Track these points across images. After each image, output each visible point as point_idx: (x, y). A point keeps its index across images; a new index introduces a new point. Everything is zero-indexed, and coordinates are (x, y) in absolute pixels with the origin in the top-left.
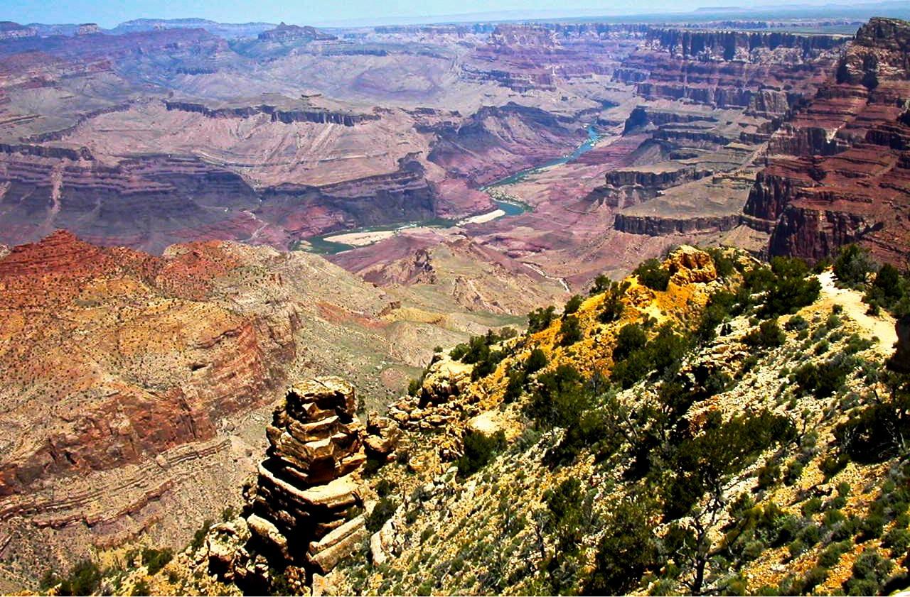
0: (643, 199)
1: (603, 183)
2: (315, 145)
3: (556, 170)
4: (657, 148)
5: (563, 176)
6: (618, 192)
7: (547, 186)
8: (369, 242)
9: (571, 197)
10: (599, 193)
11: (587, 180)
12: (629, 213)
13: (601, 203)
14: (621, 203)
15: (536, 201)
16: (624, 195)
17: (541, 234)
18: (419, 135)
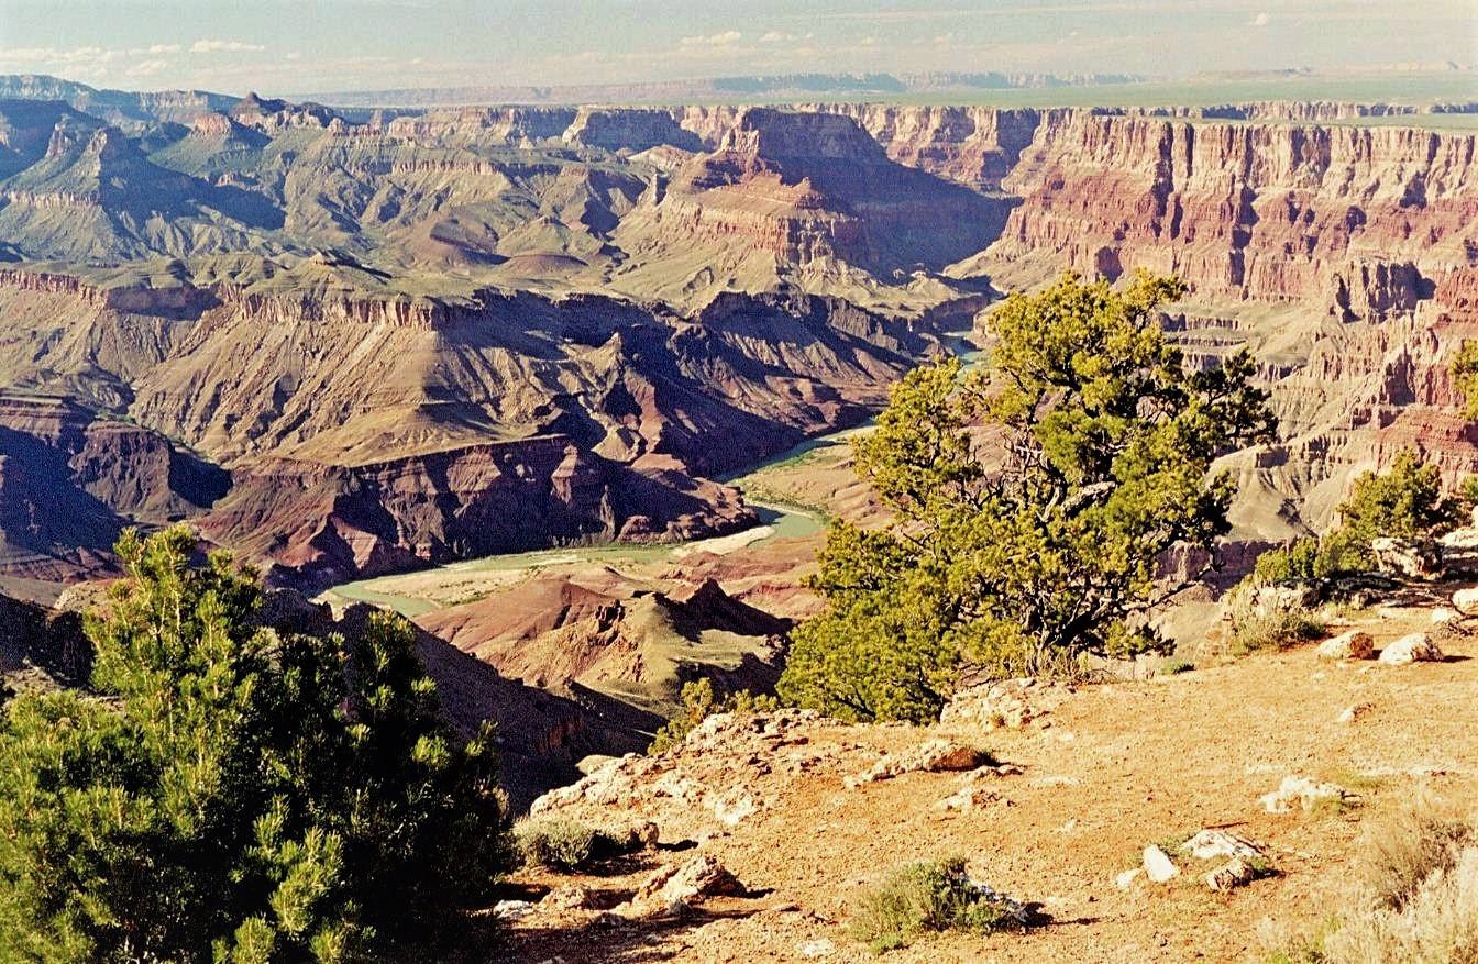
15: (845, 505)
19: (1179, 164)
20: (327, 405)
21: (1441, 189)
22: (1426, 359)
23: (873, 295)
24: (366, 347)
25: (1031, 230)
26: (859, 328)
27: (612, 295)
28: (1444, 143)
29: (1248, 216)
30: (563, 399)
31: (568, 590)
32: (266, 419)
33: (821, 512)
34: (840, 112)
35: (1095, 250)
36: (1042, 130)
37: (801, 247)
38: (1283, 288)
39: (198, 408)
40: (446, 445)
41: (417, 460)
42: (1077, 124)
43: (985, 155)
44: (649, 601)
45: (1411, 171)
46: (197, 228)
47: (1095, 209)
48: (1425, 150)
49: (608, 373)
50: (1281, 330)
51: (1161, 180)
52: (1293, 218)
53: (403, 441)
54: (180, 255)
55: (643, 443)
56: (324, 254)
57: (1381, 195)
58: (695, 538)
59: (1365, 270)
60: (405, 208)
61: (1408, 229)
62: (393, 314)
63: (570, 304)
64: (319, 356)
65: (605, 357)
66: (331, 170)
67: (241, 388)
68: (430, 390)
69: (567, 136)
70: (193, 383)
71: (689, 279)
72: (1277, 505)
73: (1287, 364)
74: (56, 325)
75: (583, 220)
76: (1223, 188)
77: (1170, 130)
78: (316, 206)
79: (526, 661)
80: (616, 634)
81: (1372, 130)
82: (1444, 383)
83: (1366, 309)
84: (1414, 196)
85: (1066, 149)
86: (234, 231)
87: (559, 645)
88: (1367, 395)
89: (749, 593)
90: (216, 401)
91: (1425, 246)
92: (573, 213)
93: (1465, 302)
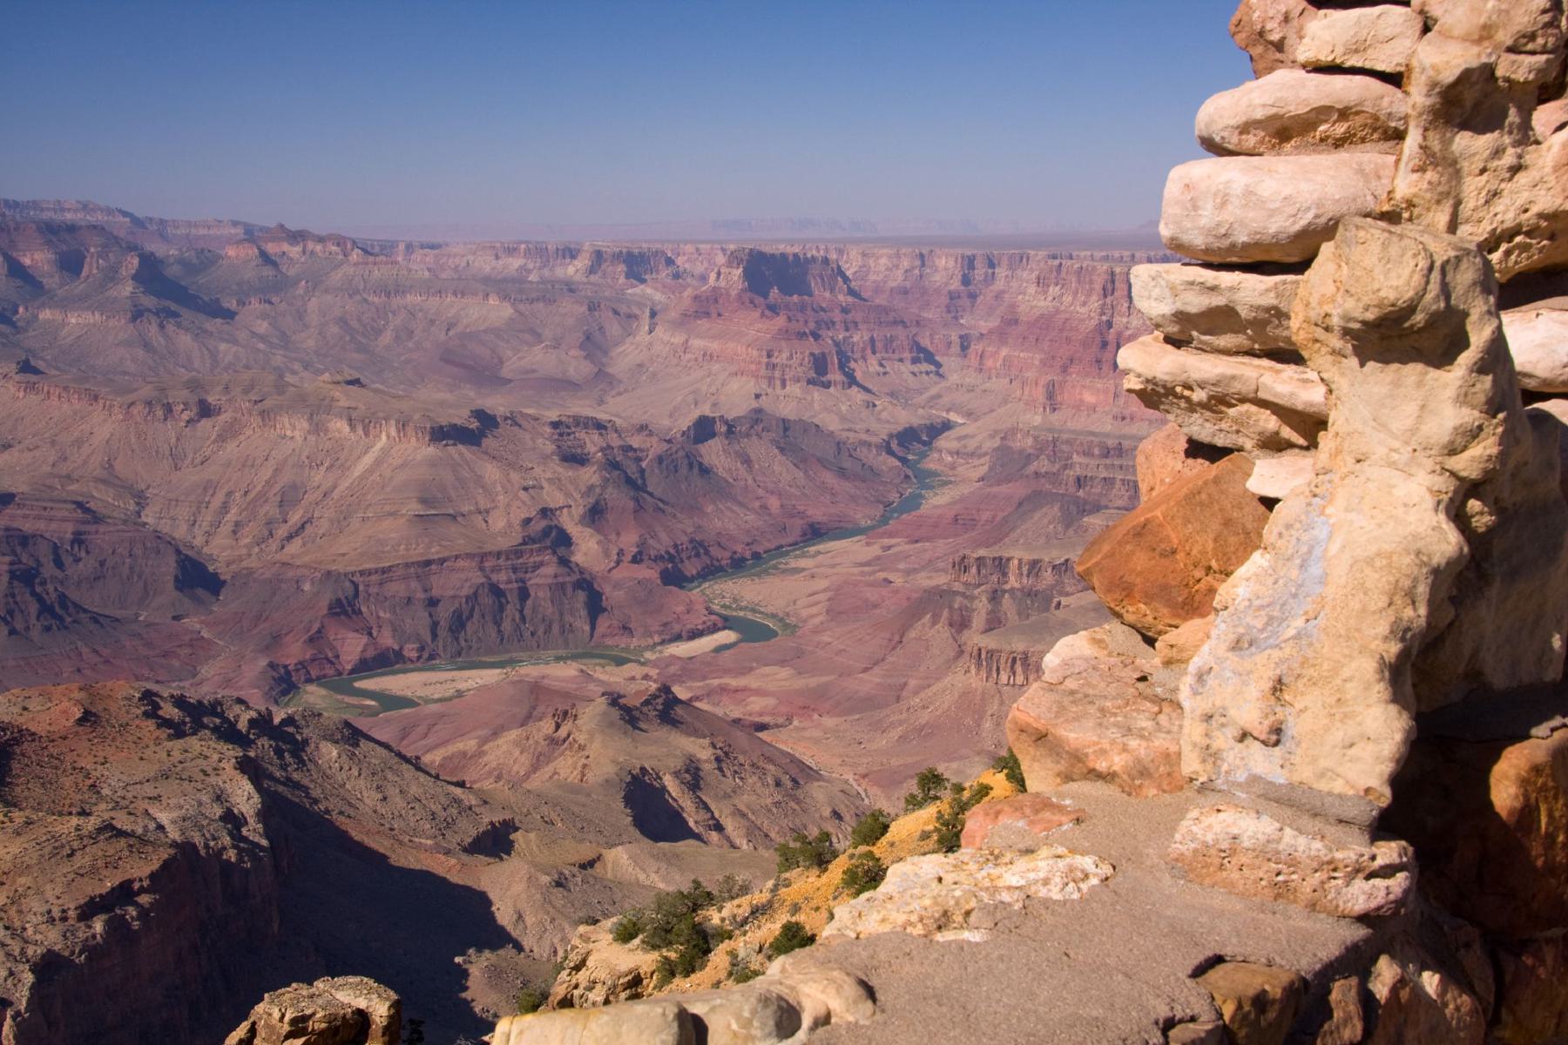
0: (1023, 614)
1: (941, 580)
2: (344, 484)
3: (843, 557)
4: (1055, 510)
5: (862, 565)
6: (972, 598)
7: (823, 584)
8: (451, 692)
9: (876, 606)
10: (932, 601)
11: (908, 572)
12: (988, 642)
13: (934, 623)
14: (978, 621)
15: (804, 613)
16: (982, 606)
17: (813, 682)
18: (565, 472)
24: (367, 460)
25: (989, 363)
30: (545, 512)
36: (1001, 272)
37: (777, 374)
39: (207, 518)
40: (435, 552)
43: (950, 293)
49: (591, 488)
51: (1104, 318)
55: (621, 553)
58: (663, 642)
62: (393, 433)
65: (589, 475)
67: (252, 495)
68: (423, 501)
69: (571, 270)
70: (205, 489)
75: (582, 347)
87: (517, 743)
89: (708, 695)
90: (225, 508)
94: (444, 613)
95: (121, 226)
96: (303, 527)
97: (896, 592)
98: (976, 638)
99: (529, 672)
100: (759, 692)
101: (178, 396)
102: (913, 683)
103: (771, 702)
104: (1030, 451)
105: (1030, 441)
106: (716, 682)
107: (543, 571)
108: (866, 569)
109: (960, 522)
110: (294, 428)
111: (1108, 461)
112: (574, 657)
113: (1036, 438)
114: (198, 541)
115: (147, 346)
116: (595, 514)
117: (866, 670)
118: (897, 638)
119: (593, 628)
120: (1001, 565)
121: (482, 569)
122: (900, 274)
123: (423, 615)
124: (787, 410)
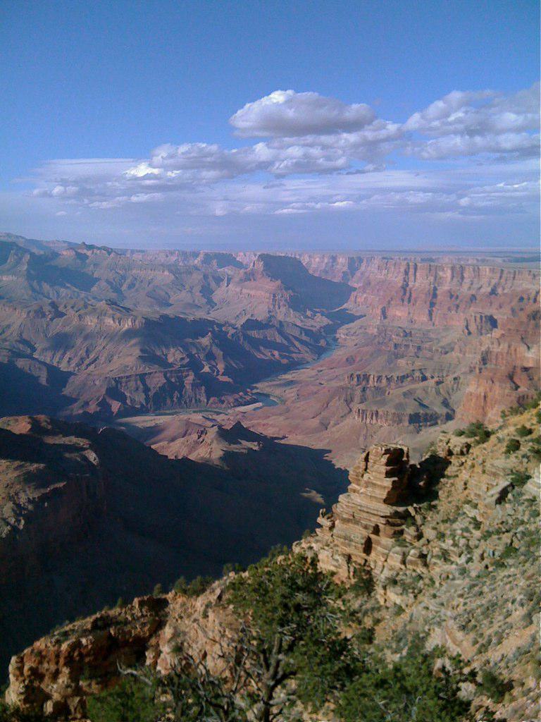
9: (316, 393)
14: (357, 399)
15: (288, 396)
16: (358, 392)
19: (412, 278)
20: (105, 355)
21: (504, 289)
22: (496, 349)
23: (302, 321)
25: (358, 300)
26: (296, 333)
27: (209, 319)
28: (505, 272)
29: (435, 296)
31: (188, 423)
32: (82, 360)
33: (280, 398)
34: (293, 256)
35: (380, 307)
36: (364, 265)
38: (447, 322)
40: (147, 370)
41: (137, 375)
42: (376, 262)
44: (216, 429)
45: (494, 282)
46: (62, 290)
47: (381, 293)
48: (499, 275)
50: (445, 337)
52: (451, 298)
53: (132, 368)
54: (55, 300)
56: (106, 301)
57: (483, 290)
58: (235, 406)
59: (475, 317)
60: (137, 285)
61: (491, 303)
63: (194, 321)
64: (103, 337)
65: (205, 341)
66: (111, 271)
71: (237, 314)
72: (441, 399)
73: (447, 350)
74: (7, 323)
76: (427, 286)
77: (409, 265)
78: (105, 283)
79: (171, 449)
80: (203, 440)
81: (480, 267)
82: (502, 359)
83: (476, 331)
84: (493, 292)
85: (372, 270)
86: (75, 291)
88: (474, 361)
89: (253, 426)
91: (497, 309)
92: (197, 290)
93: (510, 330)
94: (151, 394)
95: (21, 243)
96: (95, 360)
97: (324, 388)
98: (356, 406)
99: (184, 417)
100: (271, 425)
101: (47, 309)
102: (332, 423)
103: (274, 430)
104: (376, 334)
105: (376, 330)
106: (256, 422)
107: (188, 378)
108: (312, 379)
109: (350, 361)
110: (91, 322)
111: (406, 338)
112: (200, 411)
113: (378, 329)
114: (55, 364)
115: (33, 290)
116: (210, 356)
117: (313, 418)
118: (325, 405)
119: (208, 400)
120: (366, 378)
121: (165, 377)
122: (324, 265)
123: (143, 396)
124: (280, 317)
